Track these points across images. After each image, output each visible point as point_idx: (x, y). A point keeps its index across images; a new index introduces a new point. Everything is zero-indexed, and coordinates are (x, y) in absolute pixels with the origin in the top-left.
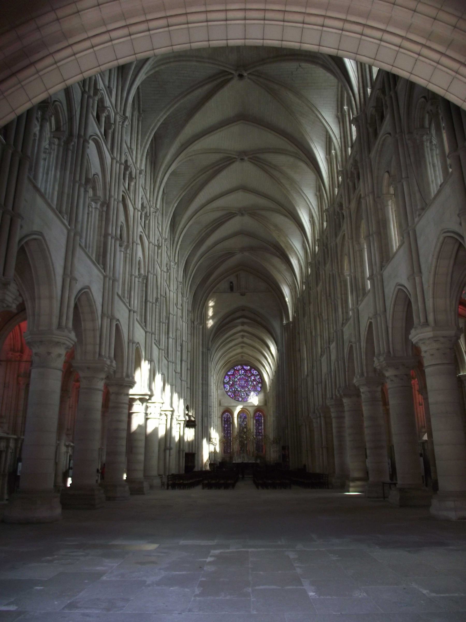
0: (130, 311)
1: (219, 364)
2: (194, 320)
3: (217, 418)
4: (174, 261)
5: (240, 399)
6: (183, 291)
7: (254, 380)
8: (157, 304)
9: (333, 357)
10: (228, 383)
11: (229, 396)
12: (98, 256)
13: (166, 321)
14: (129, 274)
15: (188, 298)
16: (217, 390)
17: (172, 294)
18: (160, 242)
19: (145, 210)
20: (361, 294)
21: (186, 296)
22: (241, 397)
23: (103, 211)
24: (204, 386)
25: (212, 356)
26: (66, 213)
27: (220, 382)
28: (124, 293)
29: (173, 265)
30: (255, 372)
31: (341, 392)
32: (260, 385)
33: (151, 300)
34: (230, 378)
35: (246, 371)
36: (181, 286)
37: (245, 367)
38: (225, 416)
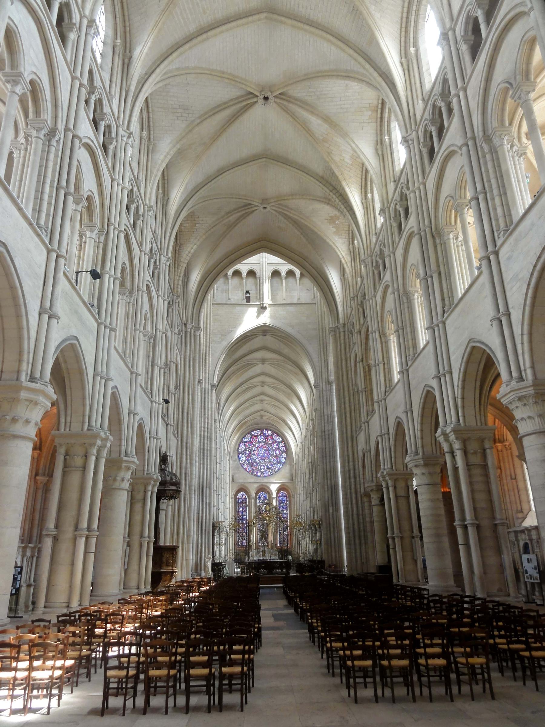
1: (232, 424)
2: (187, 321)
3: (228, 498)
4: (128, 128)
5: (259, 474)
6: (161, 245)
7: (277, 449)
10: (243, 453)
11: (245, 469)
13: (99, 238)
15: (169, 258)
16: (229, 460)
21: (167, 255)
22: (260, 472)
24: (206, 439)
25: (222, 407)
27: (234, 452)
29: (124, 136)
30: (278, 437)
32: (284, 455)
34: (246, 446)
35: (267, 436)
36: (150, 214)
37: (265, 432)
38: (239, 496)
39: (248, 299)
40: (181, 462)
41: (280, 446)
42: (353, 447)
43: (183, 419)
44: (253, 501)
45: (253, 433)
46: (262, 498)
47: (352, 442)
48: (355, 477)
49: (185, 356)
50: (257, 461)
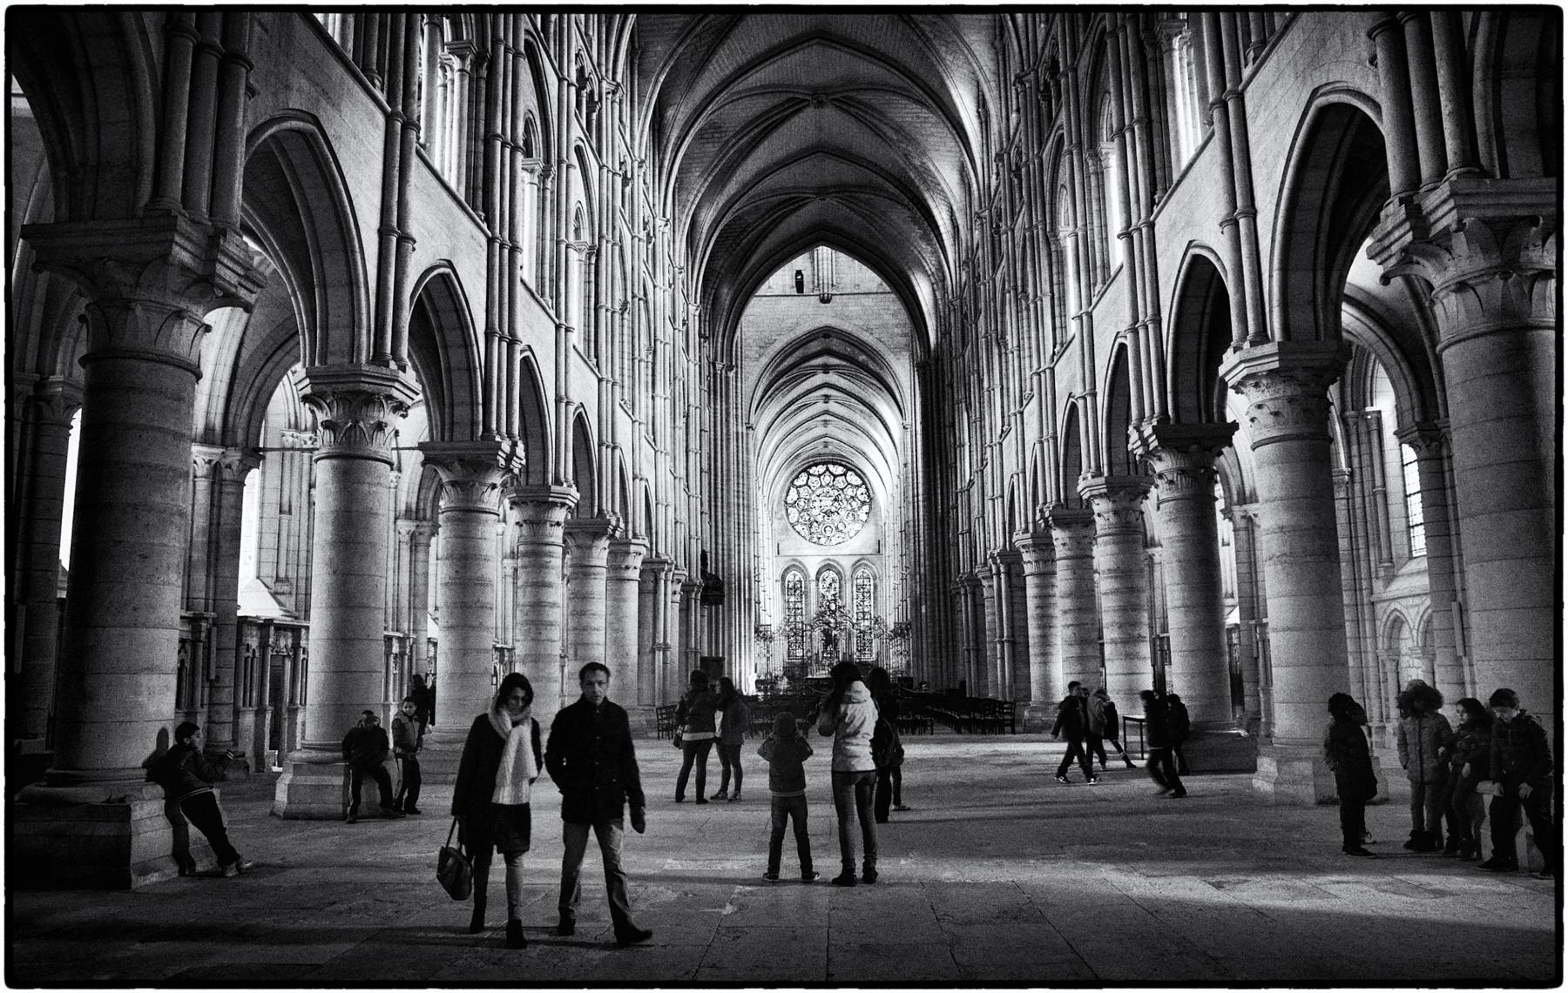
0: (558, 327)
8: (626, 316)
9: (1032, 435)
10: (794, 504)
12: (471, 189)
14: (552, 240)
17: (659, 293)
18: (629, 168)
19: (588, 88)
20: (1099, 279)
23: (479, 79)
26: (381, 74)
28: (543, 286)
31: (1047, 514)
32: (866, 508)
33: (609, 305)
35: (835, 476)
38: (789, 577)
39: (800, 286)
40: (717, 554)
41: (859, 493)
42: (943, 533)
43: (716, 497)
44: (813, 585)
45: (811, 471)
46: (829, 581)
47: (943, 526)
48: (944, 574)
49: (715, 409)
50: (820, 518)
